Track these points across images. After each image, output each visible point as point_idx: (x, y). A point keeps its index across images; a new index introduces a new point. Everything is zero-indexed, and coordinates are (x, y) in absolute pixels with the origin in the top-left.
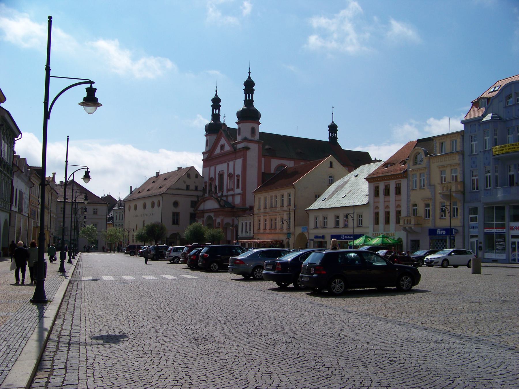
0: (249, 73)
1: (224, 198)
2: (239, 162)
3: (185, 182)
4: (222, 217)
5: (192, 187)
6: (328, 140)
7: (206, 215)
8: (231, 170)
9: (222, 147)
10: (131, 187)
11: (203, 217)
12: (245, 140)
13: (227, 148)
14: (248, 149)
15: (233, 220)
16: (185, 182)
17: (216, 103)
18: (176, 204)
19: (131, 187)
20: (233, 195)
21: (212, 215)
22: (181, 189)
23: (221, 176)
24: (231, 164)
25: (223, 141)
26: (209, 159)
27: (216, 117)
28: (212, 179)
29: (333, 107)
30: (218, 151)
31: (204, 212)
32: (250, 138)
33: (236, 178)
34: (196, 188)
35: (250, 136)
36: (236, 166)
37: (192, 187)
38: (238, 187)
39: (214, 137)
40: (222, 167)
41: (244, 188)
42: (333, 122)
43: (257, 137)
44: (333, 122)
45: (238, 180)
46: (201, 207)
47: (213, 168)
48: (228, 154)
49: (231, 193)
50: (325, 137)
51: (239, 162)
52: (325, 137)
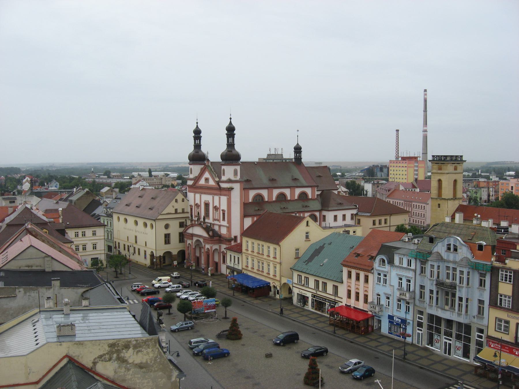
3: (173, 207)
5: (180, 210)
7: (195, 239)
8: (216, 204)
9: (207, 180)
11: (192, 239)
12: (230, 181)
15: (220, 246)
16: (173, 207)
18: (167, 227)
21: (202, 240)
32: (233, 178)
33: (221, 212)
37: (180, 210)
41: (229, 222)
45: (224, 214)
46: (190, 231)
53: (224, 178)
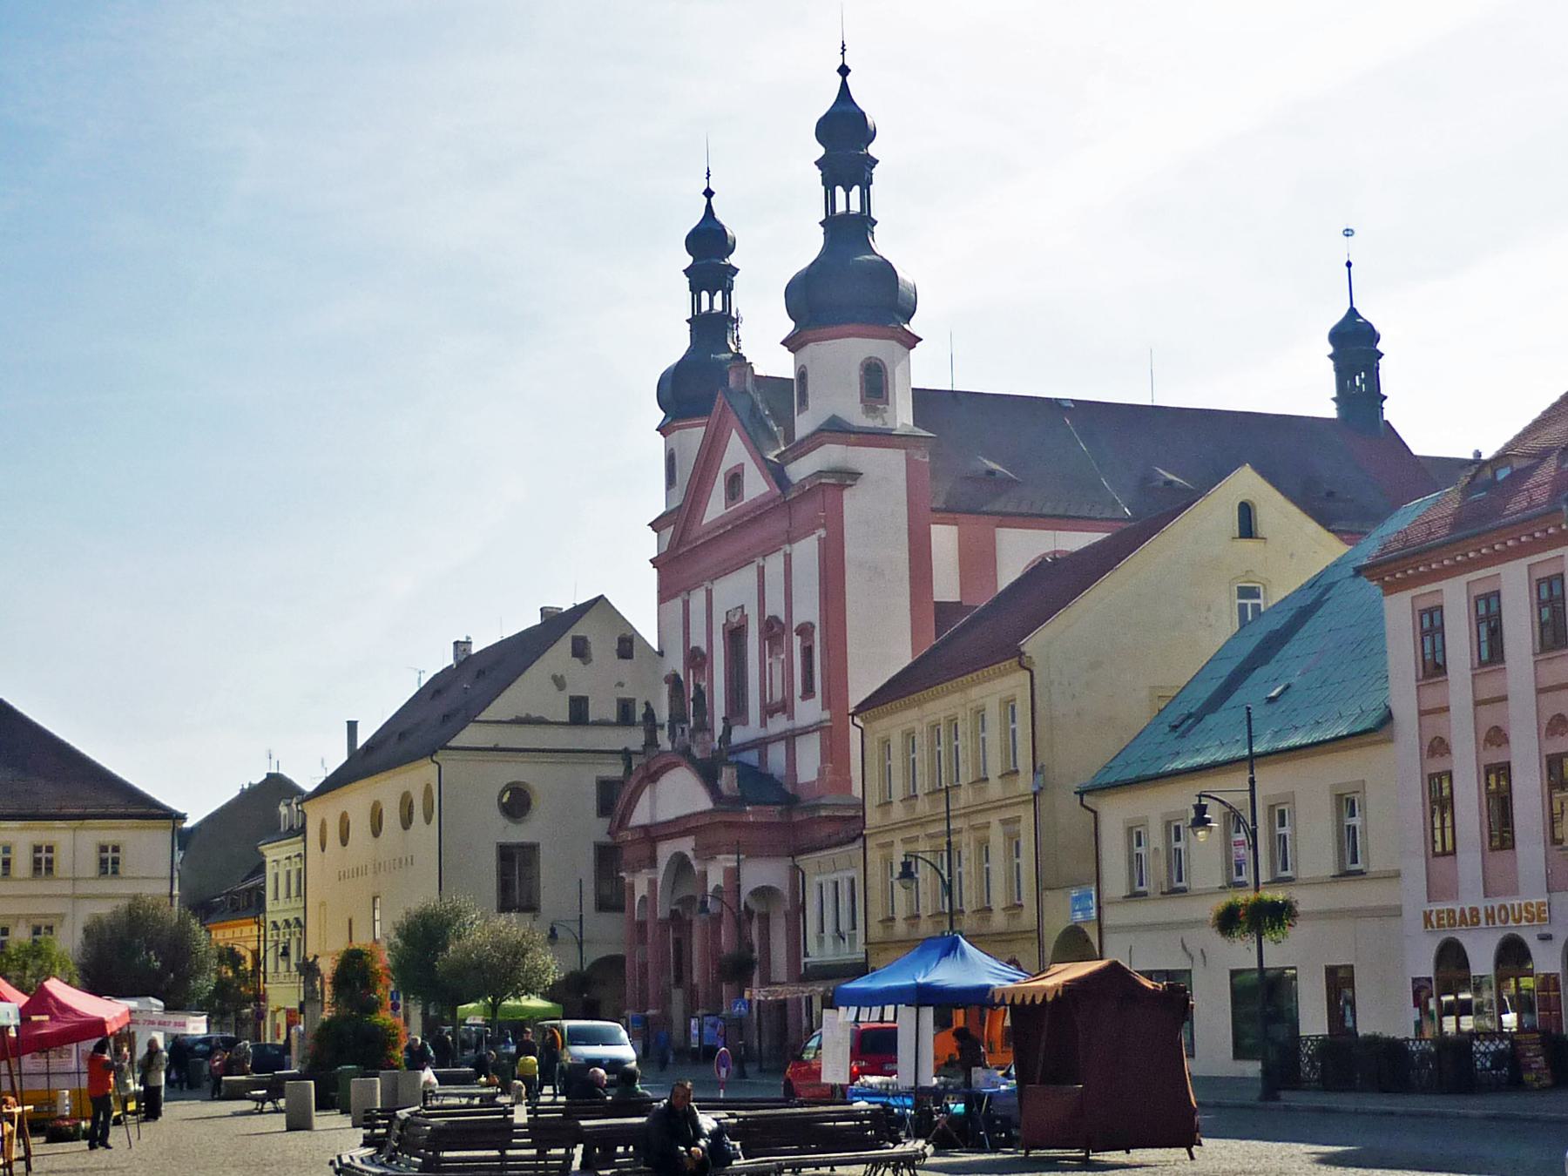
0: (844, 71)
1: (751, 757)
2: (806, 551)
3: (559, 682)
4: (727, 861)
5: (603, 707)
6: (1330, 411)
7: (665, 851)
8: (775, 607)
9: (735, 481)
10: (352, 727)
11: (652, 862)
12: (835, 430)
13: (756, 486)
14: (846, 477)
17: (710, 252)
18: (517, 803)
19: (352, 727)
20: (790, 738)
22: (540, 722)
23: (735, 635)
24: (774, 564)
25: (736, 451)
26: (683, 556)
27: (712, 330)
28: (697, 660)
29: (1348, 233)
30: (716, 508)
31: (653, 834)
32: (858, 417)
33: (797, 640)
34: (625, 707)
35: (859, 407)
36: (788, 580)
37: (603, 707)
38: (808, 692)
39: (693, 436)
40: (734, 592)
42: (1353, 312)
43: (902, 416)
44: (1353, 312)
45: (808, 653)
46: (641, 815)
47: (698, 599)
48: (760, 513)
49: (779, 724)
50: (1310, 391)
51: (806, 551)
52: (1310, 391)
53: (804, 425)
